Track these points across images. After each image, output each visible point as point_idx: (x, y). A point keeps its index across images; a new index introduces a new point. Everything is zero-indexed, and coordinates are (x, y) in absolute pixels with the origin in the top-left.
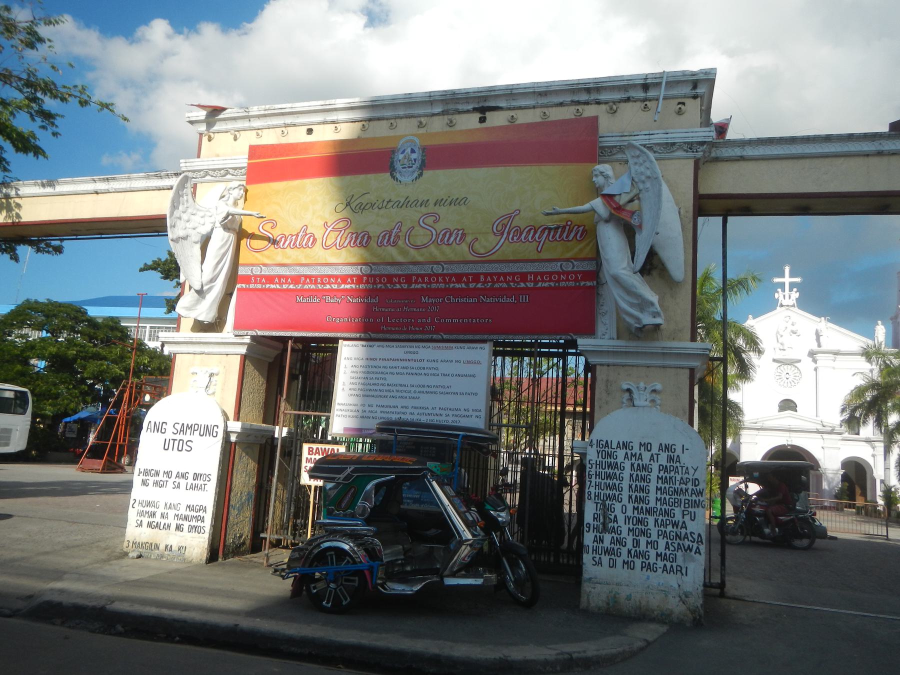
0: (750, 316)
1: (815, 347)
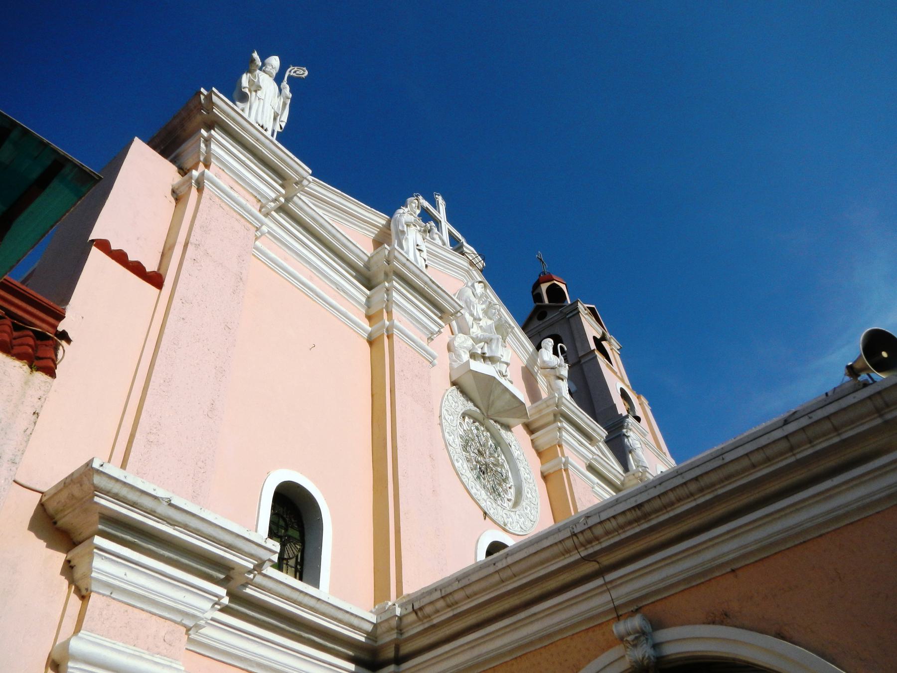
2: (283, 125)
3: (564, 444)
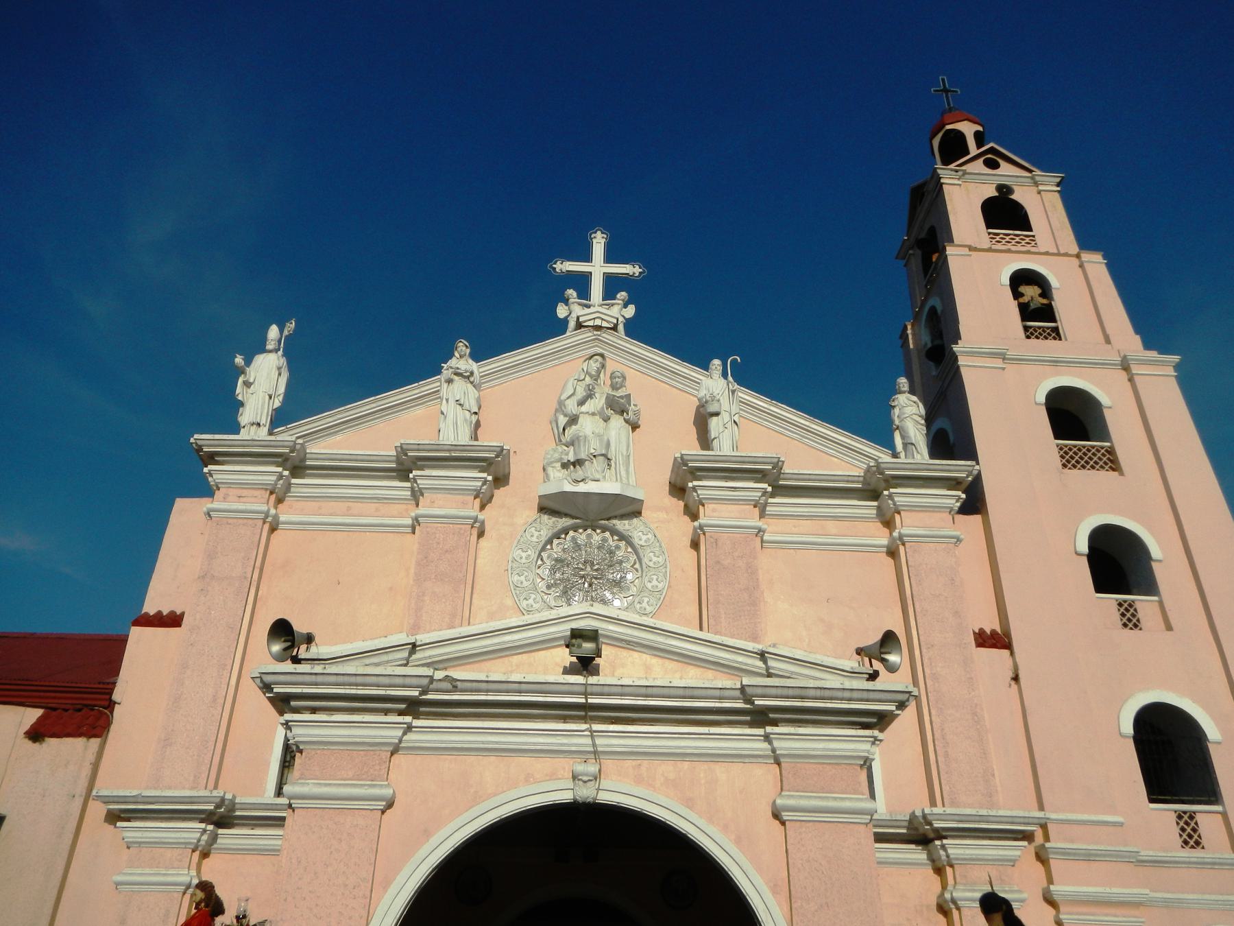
0: (462, 347)
1: (691, 448)
2: (281, 398)
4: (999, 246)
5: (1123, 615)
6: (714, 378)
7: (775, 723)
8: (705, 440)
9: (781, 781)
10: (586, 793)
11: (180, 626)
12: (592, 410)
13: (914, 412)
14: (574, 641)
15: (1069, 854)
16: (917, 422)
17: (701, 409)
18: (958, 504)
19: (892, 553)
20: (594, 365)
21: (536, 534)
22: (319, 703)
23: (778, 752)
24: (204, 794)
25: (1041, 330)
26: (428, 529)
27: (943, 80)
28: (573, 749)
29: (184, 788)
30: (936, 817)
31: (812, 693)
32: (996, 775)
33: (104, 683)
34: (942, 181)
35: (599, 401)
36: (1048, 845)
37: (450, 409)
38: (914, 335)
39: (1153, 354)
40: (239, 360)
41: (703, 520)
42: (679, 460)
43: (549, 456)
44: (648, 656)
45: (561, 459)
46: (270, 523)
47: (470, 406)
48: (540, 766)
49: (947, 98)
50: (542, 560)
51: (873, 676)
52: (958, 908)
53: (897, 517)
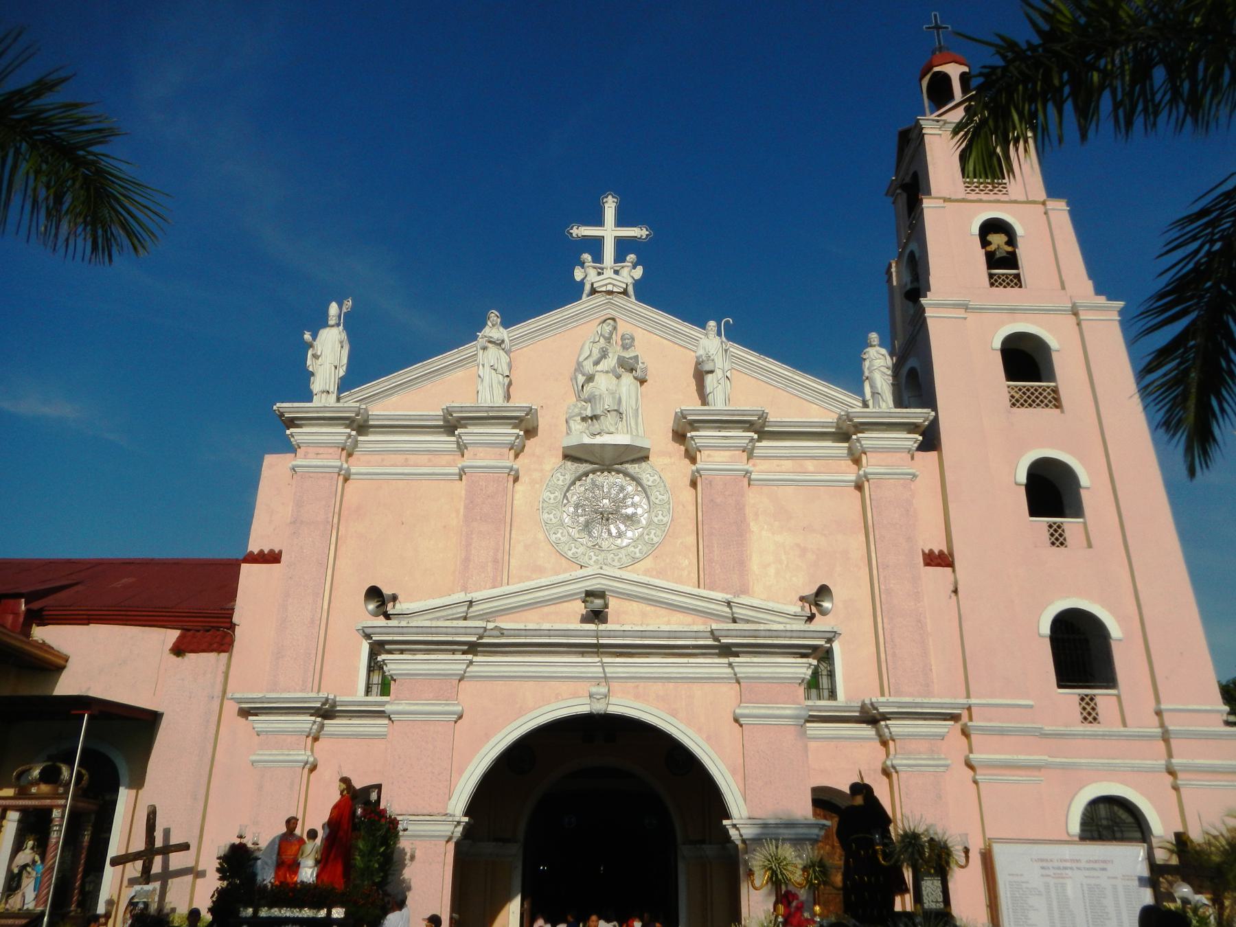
0: (494, 316)
1: (692, 404)
2: (344, 368)
3: (700, 448)
4: (973, 196)
5: (1052, 535)
6: (710, 338)
7: (737, 655)
8: (703, 397)
9: (741, 695)
10: (599, 707)
11: (279, 562)
12: (606, 369)
13: (882, 364)
14: (587, 599)
15: (987, 730)
16: (885, 373)
17: (699, 366)
18: (916, 445)
19: (859, 487)
20: (607, 328)
21: (562, 478)
22: (405, 647)
23: (738, 675)
24: (314, 697)
25: (1004, 277)
26: (473, 478)
27: (935, 16)
28: (590, 675)
29: (295, 691)
30: (881, 704)
31: (763, 634)
32: (933, 670)
33: (225, 610)
34: (924, 131)
35: (612, 360)
36: (970, 724)
37: (486, 372)
38: (897, 272)
39: (1102, 300)
40: (307, 336)
41: (699, 466)
42: (679, 414)
43: (570, 411)
44: (643, 605)
45: (580, 414)
46: (344, 476)
47: (502, 371)
48: (565, 687)
49: (938, 35)
50: (567, 499)
51: (811, 618)
52: (897, 772)
53: (864, 457)
